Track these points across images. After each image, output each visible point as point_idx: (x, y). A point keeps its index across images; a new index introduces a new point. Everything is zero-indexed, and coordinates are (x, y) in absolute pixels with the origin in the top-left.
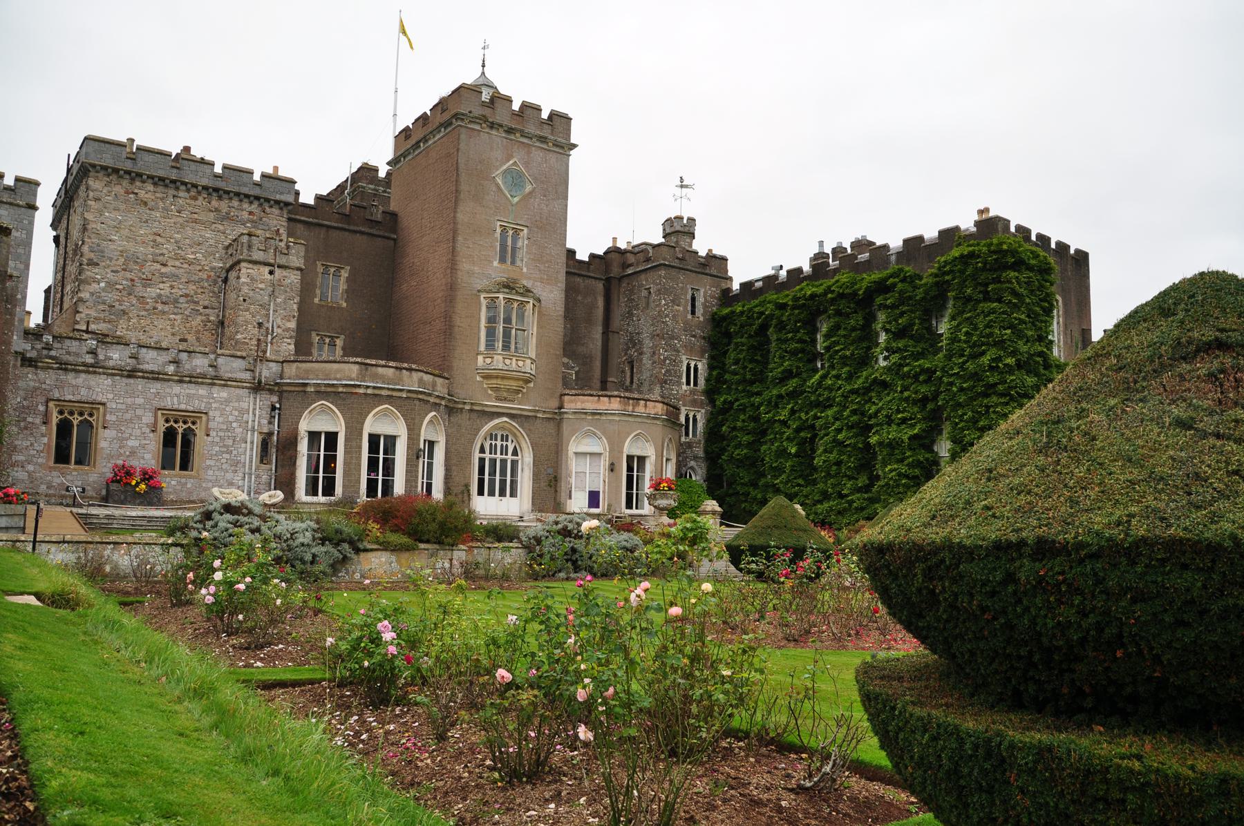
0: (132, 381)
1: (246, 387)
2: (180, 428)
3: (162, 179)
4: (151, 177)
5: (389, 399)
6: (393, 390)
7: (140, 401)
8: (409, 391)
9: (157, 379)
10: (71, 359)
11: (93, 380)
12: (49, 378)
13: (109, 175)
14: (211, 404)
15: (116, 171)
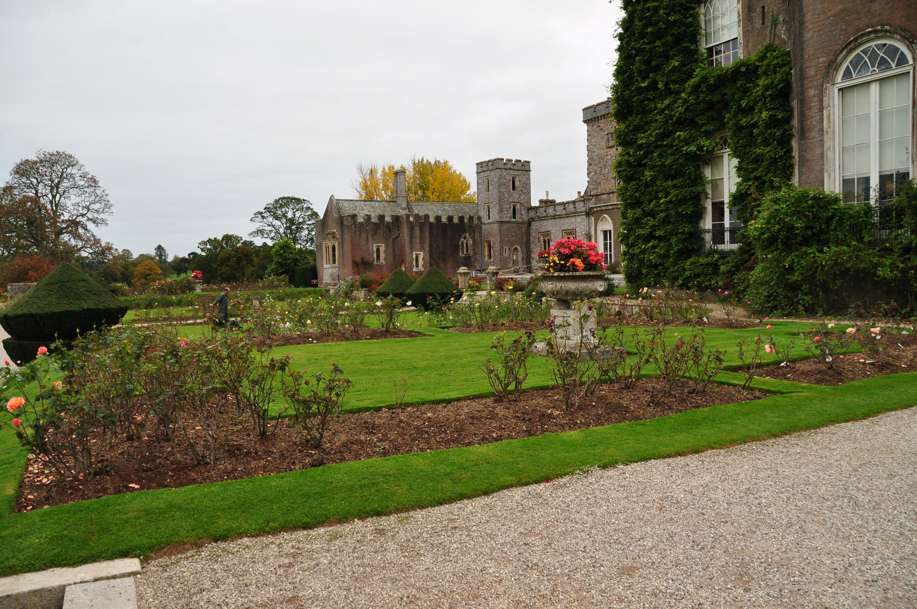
3: (604, 115)
4: (601, 116)
5: (606, 211)
6: (607, 206)
7: (558, 228)
8: (610, 205)
9: (561, 218)
10: (541, 215)
11: (544, 223)
12: (538, 223)
15: (591, 119)
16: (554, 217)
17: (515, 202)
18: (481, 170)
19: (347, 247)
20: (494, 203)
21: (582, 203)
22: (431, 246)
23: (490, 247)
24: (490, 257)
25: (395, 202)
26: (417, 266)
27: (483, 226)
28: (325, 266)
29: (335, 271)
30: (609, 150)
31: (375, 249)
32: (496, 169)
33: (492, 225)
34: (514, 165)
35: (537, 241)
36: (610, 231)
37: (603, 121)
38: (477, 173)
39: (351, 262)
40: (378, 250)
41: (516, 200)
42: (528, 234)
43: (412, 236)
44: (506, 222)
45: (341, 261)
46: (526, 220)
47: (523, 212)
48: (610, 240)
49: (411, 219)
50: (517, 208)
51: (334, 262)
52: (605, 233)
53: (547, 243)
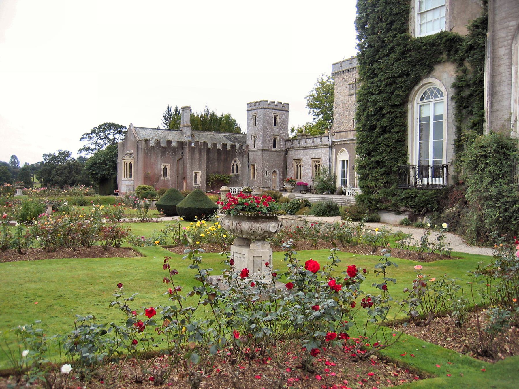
0: (306, 150)
1: (327, 147)
2: (317, 164)
6: (345, 141)
7: (308, 157)
9: (311, 149)
10: (295, 146)
11: (298, 152)
13: (338, 75)
14: (321, 155)
16: (306, 148)
17: (275, 135)
18: (250, 108)
19: (141, 164)
20: (259, 136)
21: (327, 138)
22: (207, 167)
23: (254, 169)
24: (254, 177)
25: (182, 131)
26: (196, 182)
27: (250, 153)
28: (123, 179)
29: (131, 183)
30: (350, 97)
31: (163, 167)
32: (262, 108)
33: (257, 152)
34: (276, 106)
35: (292, 166)
36: (347, 161)
37: (347, 74)
38: (247, 111)
39: (143, 177)
40: (165, 168)
41: (276, 134)
42: (285, 161)
43: (192, 158)
44: (268, 150)
45: (136, 176)
46: (284, 149)
47: (282, 143)
48: (347, 168)
49: (193, 145)
50: (277, 139)
51: (130, 176)
52: (343, 162)
53: (299, 168)
